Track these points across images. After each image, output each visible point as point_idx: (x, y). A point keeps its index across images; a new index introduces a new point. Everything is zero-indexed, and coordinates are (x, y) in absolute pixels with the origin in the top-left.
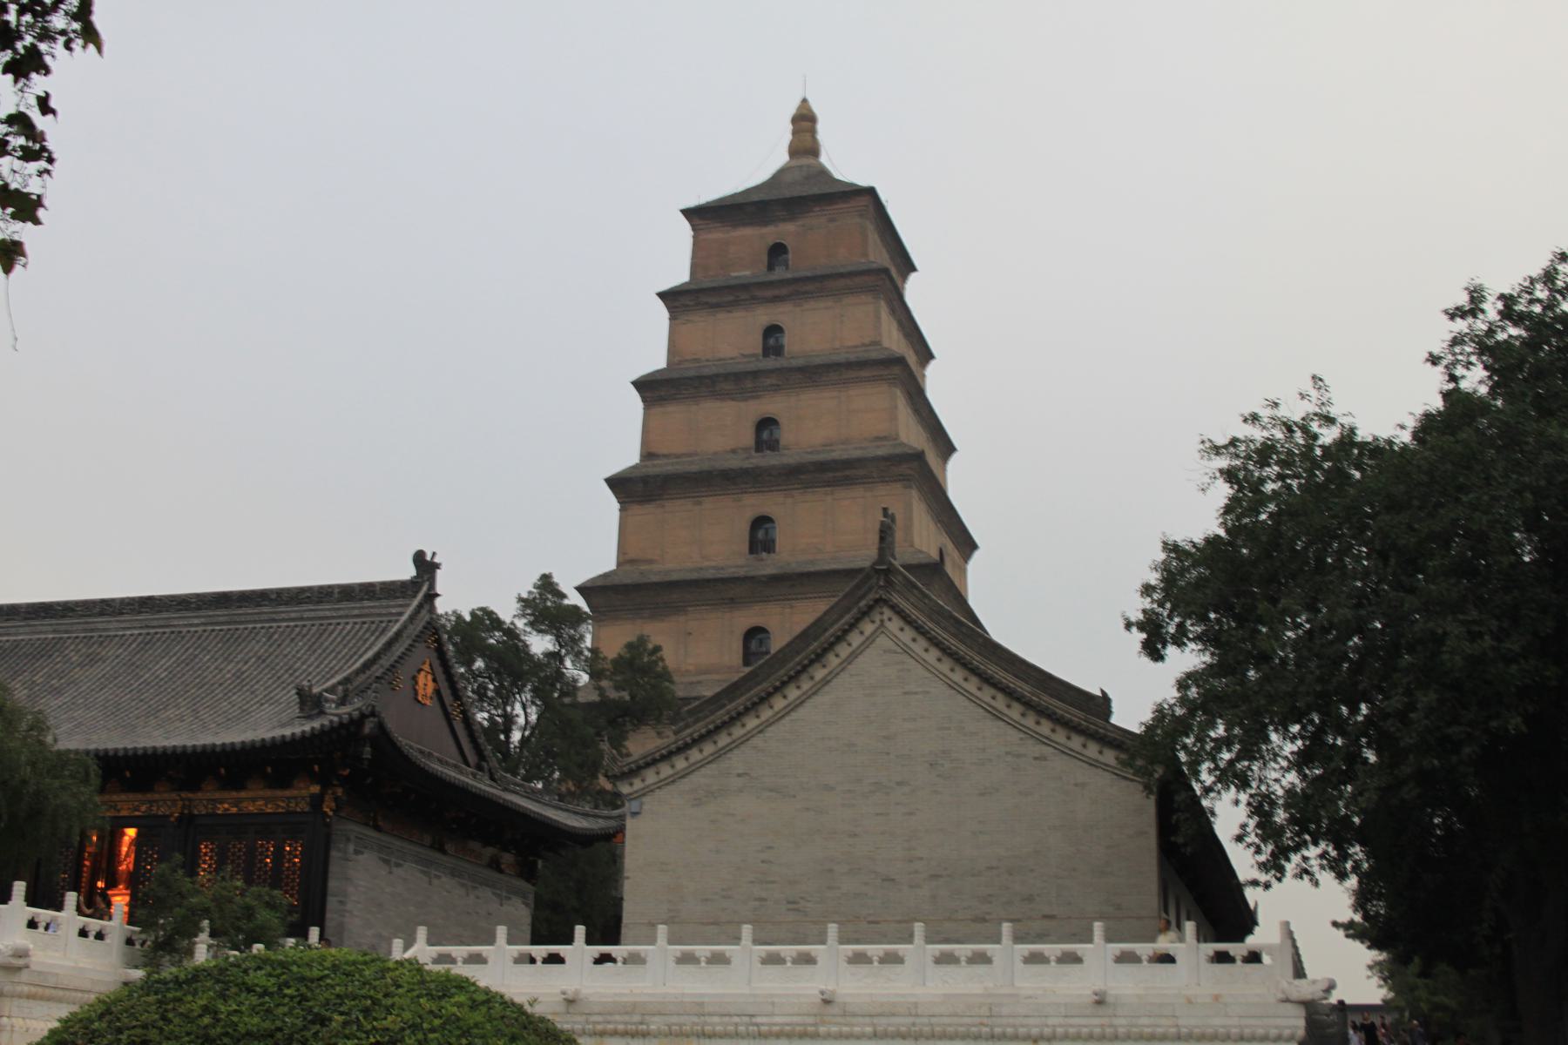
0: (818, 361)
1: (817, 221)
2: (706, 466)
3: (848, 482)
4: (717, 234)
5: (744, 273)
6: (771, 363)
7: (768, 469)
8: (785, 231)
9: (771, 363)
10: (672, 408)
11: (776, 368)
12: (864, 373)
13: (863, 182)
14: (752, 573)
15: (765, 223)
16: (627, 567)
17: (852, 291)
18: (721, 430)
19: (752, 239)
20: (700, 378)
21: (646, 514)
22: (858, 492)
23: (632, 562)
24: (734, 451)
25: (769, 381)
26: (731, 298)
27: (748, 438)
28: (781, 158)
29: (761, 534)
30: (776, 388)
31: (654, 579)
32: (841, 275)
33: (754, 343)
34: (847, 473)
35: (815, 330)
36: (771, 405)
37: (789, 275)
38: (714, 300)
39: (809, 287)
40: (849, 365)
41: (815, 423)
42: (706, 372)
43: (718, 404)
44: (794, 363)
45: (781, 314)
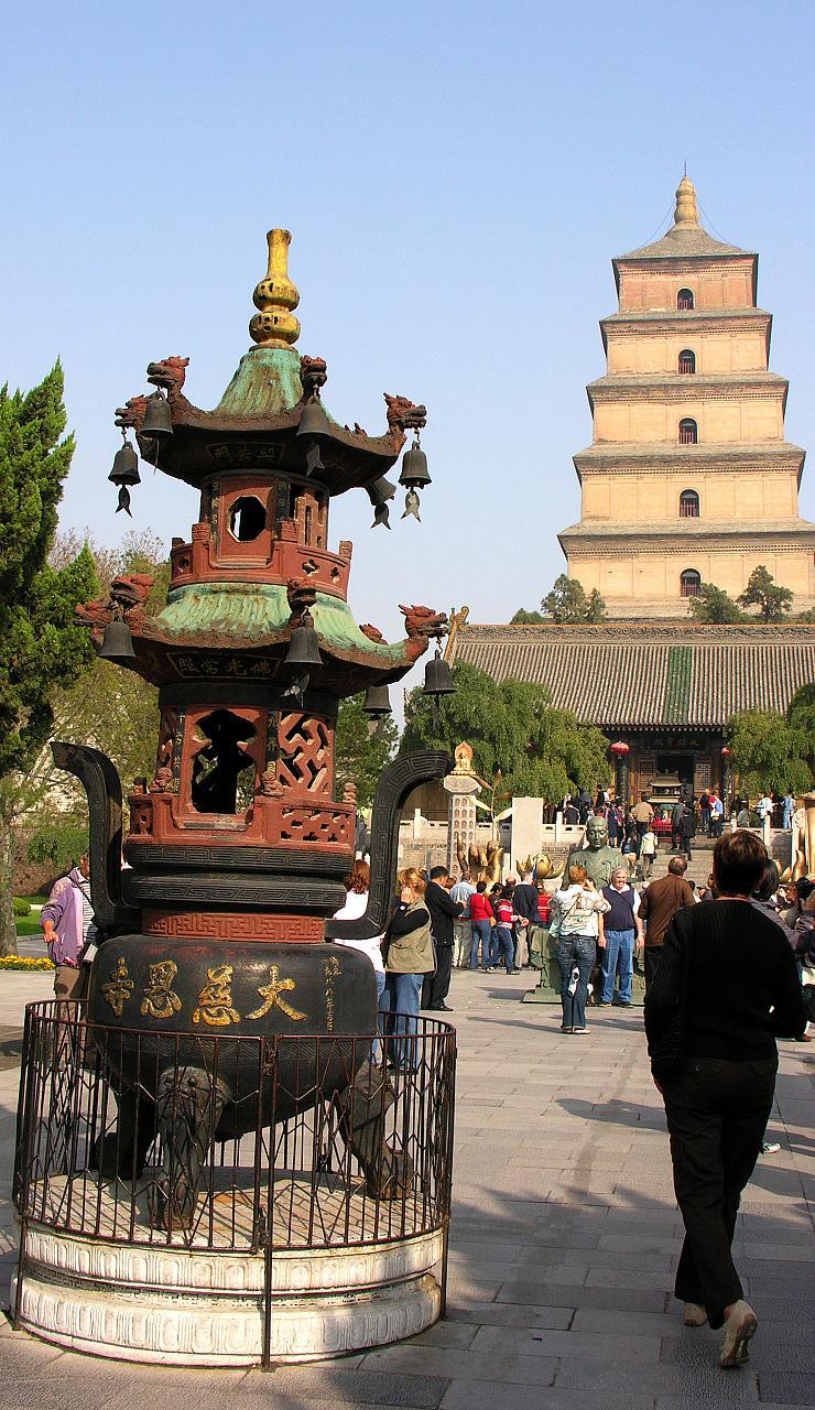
0: (724, 380)
2: (647, 452)
3: (751, 469)
5: (660, 310)
6: (686, 378)
8: (688, 280)
10: (616, 407)
14: (688, 532)
15: (675, 274)
16: (588, 523)
17: (743, 329)
18: (651, 425)
20: (639, 387)
21: (597, 484)
22: (757, 476)
23: (593, 518)
24: (663, 441)
27: (675, 432)
30: (695, 397)
31: (615, 532)
32: (738, 318)
33: (674, 363)
35: (721, 354)
36: (690, 410)
37: (699, 315)
39: (714, 324)
40: (749, 385)
41: (723, 424)
42: (641, 382)
43: (654, 406)
44: (707, 380)
45: (692, 342)
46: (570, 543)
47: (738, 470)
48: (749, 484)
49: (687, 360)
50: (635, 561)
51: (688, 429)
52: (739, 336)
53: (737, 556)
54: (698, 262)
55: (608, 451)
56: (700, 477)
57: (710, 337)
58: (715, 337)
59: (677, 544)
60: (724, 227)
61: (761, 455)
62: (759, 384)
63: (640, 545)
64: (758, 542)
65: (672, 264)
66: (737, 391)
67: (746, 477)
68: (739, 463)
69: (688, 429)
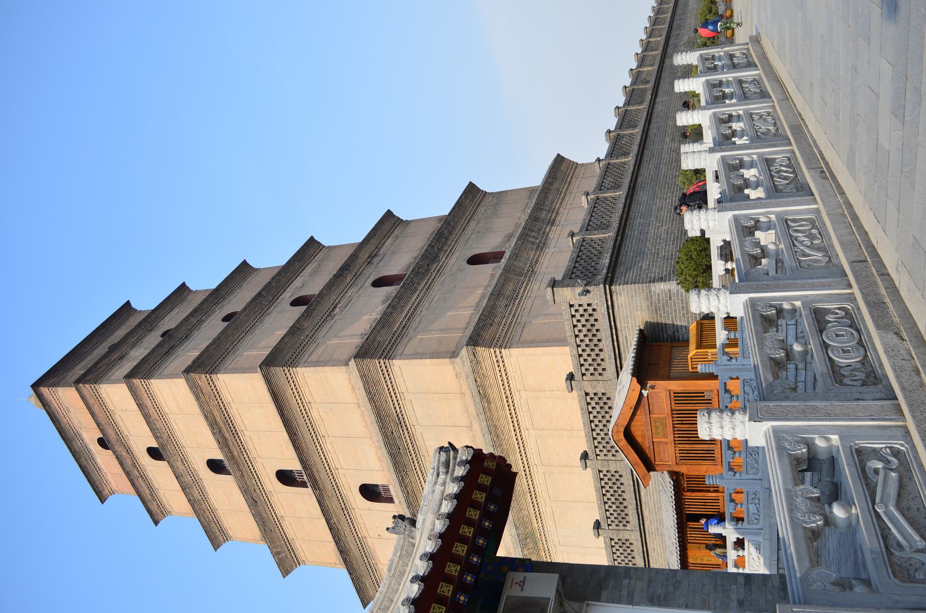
3: (229, 422)
12: (148, 403)
25: (181, 467)
26: (140, 479)
34: (221, 424)
38: (147, 492)
43: (210, 496)
47: (235, 433)
48: (246, 422)
50: (369, 540)
52: (111, 407)
53: (328, 447)
56: (259, 467)
57: (126, 433)
58: (123, 429)
59: (333, 505)
61: (206, 417)
62: (141, 406)
63: (350, 538)
64: (303, 431)
66: (159, 425)
67: (239, 424)
68: (227, 435)
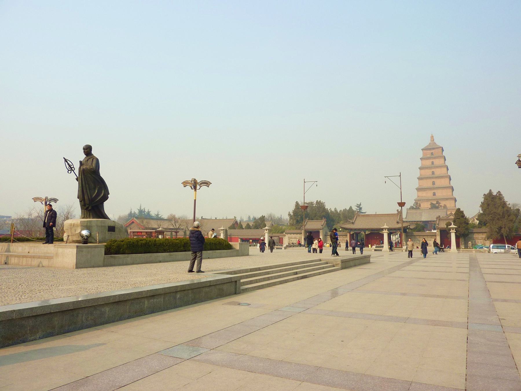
1: (436, 150)
4: (425, 151)
6: (433, 166)
7: (433, 177)
8: (433, 151)
9: (433, 166)
11: (433, 166)
13: (441, 146)
18: (428, 173)
19: (429, 152)
28: (430, 142)
29: (434, 183)
35: (437, 162)
36: (433, 170)
41: (438, 172)
45: (434, 160)
46: (418, 190)
49: (433, 163)
51: (433, 173)
54: (434, 149)
55: (422, 177)
60: (439, 142)
65: (430, 149)
69: (433, 173)
